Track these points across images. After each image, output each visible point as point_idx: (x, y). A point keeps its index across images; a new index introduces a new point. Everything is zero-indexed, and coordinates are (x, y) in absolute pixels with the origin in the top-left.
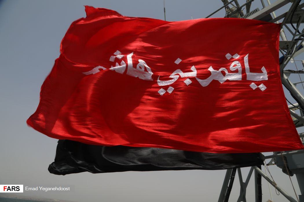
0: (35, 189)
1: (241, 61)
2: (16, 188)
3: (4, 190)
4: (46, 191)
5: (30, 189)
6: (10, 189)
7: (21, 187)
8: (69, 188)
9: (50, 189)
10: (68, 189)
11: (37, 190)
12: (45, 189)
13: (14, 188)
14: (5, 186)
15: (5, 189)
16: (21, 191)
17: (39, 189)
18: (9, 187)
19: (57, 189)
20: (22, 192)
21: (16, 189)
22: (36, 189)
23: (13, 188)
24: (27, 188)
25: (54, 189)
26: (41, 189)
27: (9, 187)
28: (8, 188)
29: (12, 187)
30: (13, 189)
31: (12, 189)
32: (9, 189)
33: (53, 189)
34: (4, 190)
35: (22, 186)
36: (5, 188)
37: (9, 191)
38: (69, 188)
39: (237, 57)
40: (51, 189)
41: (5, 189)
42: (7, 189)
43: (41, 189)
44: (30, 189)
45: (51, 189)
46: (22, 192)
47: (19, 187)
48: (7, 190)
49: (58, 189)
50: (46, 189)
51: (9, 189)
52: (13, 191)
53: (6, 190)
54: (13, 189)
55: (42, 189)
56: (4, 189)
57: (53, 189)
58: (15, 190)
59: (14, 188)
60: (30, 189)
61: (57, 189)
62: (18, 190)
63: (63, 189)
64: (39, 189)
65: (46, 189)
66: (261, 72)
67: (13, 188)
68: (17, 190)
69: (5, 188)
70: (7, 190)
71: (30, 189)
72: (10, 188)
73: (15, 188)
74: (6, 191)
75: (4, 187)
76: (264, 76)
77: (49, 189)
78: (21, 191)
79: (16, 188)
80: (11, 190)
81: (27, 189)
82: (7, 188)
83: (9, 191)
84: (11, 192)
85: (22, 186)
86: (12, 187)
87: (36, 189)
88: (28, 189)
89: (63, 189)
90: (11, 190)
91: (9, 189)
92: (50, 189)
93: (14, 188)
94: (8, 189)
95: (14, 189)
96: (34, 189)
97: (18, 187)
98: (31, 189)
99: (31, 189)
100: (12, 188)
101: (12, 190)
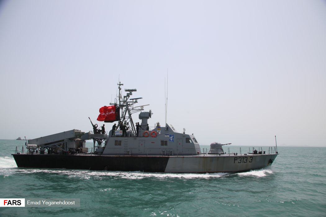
0: (37, 203)
2: (17, 202)
3: (5, 204)
4: (50, 205)
5: (32, 203)
6: (11, 203)
8: (74, 202)
9: (54, 203)
10: (73, 203)
11: (40, 204)
12: (48, 203)
13: (15, 202)
16: (23, 205)
17: (42, 203)
18: (10, 201)
19: (61, 203)
20: (24, 206)
21: (17, 203)
22: (39, 203)
24: (28, 202)
25: (58, 203)
26: (44, 203)
27: (10, 201)
28: (9, 202)
29: (13, 201)
30: (14, 204)
31: (13, 203)
32: (10, 203)
34: (5, 204)
35: (24, 199)
36: (6, 202)
42: (8, 203)
43: (44, 203)
44: (32, 203)
46: (24, 206)
47: (20, 201)
48: (8, 205)
49: (62, 203)
50: (50, 203)
51: (10, 203)
52: (14, 206)
54: (14, 204)
55: (45, 203)
56: (5, 203)
57: (57, 203)
58: (16, 205)
59: (14, 202)
60: (32, 203)
61: (61, 203)
62: (19, 204)
63: (68, 203)
64: (42, 203)
65: (50, 203)
67: (14, 202)
68: (18, 204)
69: (6, 202)
70: (8, 205)
71: (32, 203)
72: (10, 202)
73: (16, 202)
74: (6, 205)
75: (5, 201)
77: (52, 203)
79: (17, 202)
80: (11, 205)
81: (29, 203)
82: (8, 202)
83: (10, 206)
84: (12, 206)
86: (13, 201)
87: (39, 203)
88: (30, 203)
89: (68, 203)
90: (11, 205)
91: (9, 203)
92: (54, 203)
93: (15, 202)
94: (8, 203)
95: (15, 203)
96: (36, 204)
97: (19, 201)
98: (33, 203)
99: (33, 203)
100: (13, 202)
101: (13, 205)
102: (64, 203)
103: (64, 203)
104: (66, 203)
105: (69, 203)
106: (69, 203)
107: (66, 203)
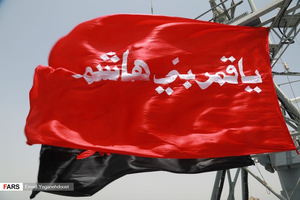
1: (235, 64)
2: (16, 186)
3: (4, 188)
4: (46, 189)
6: (10, 188)
7: (21, 185)
8: (68, 186)
10: (67, 187)
13: (14, 186)
14: (5, 184)
15: (5, 187)
18: (9, 185)
19: (56, 187)
21: (15, 187)
23: (13, 186)
24: (26, 186)
25: (53, 188)
26: (40, 187)
27: (9, 185)
28: (8, 186)
29: (12, 185)
30: (13, 188)
31: (12, 187)
32: (9, 187)
33: (52, 187)
34: (4, 188)
36: (5, 186)
37: (9, 189)
38: (68, 186)
39: (232, 59)
40: (51, 187)
41: (5, 187)
42: (7, 187)
43: (40, 187)
44: (29, 187)
45: (51, 187)
47: (19, 185)
48: (7, 189)
49: (57, 187)
50: (46, 187)
51: (9, 187)
53: (6, 188)
54: (13, 188)
55: (41, 187)
56: (4, 187)
57: (52, 187)
58: (15, 189)
59: (13, 186)
60: (29, 187)
61: (56, 187)
62: (18, 188)
63: (62, 187)
65: (46, 187)
66: (255, 75)
67: (13, 186)
68: (16, 188)
69: (5, 186)
70: (7, 189)
72: (10, 186)
73: (15, 186)
75: (4, 185)
76: (258, 79)
77: (48, 188)
78: (21, 189)
79: (16, 186)
80: (10, 189)
81: (26, 187)
82: (7, 186)
85: (22, 184)
86: (12, 185)
88: (28, 187)
89: (62, 187)
90: (10, 189)
91: (9, 187)
93: (14, 186)
94: (8, 188)
95: (14, 187)
97: (17, 186)
98: (31, 187)
99: (31, 187)
100: (12, 186)
101: (12, 189)
102: (58, 187)
103: (58, 187)
104: (61, 187)
105: (64, 187)
106: (64, 187)
107: (61, 187)
